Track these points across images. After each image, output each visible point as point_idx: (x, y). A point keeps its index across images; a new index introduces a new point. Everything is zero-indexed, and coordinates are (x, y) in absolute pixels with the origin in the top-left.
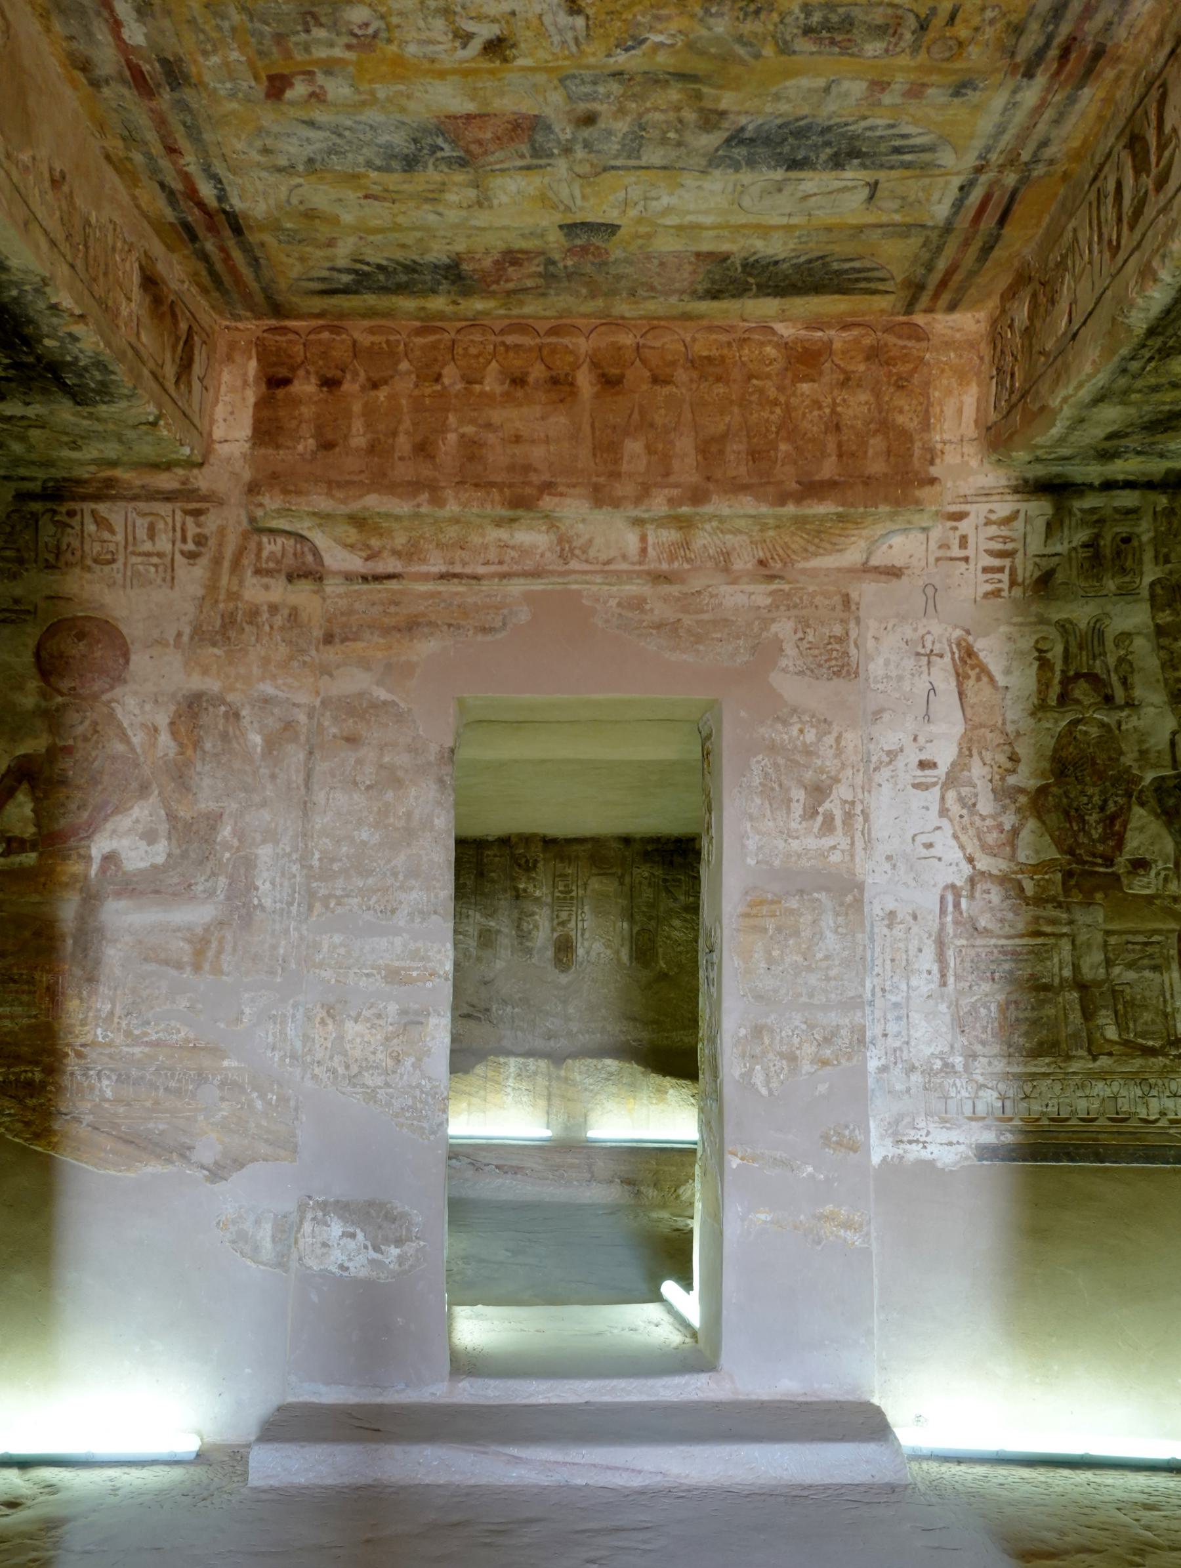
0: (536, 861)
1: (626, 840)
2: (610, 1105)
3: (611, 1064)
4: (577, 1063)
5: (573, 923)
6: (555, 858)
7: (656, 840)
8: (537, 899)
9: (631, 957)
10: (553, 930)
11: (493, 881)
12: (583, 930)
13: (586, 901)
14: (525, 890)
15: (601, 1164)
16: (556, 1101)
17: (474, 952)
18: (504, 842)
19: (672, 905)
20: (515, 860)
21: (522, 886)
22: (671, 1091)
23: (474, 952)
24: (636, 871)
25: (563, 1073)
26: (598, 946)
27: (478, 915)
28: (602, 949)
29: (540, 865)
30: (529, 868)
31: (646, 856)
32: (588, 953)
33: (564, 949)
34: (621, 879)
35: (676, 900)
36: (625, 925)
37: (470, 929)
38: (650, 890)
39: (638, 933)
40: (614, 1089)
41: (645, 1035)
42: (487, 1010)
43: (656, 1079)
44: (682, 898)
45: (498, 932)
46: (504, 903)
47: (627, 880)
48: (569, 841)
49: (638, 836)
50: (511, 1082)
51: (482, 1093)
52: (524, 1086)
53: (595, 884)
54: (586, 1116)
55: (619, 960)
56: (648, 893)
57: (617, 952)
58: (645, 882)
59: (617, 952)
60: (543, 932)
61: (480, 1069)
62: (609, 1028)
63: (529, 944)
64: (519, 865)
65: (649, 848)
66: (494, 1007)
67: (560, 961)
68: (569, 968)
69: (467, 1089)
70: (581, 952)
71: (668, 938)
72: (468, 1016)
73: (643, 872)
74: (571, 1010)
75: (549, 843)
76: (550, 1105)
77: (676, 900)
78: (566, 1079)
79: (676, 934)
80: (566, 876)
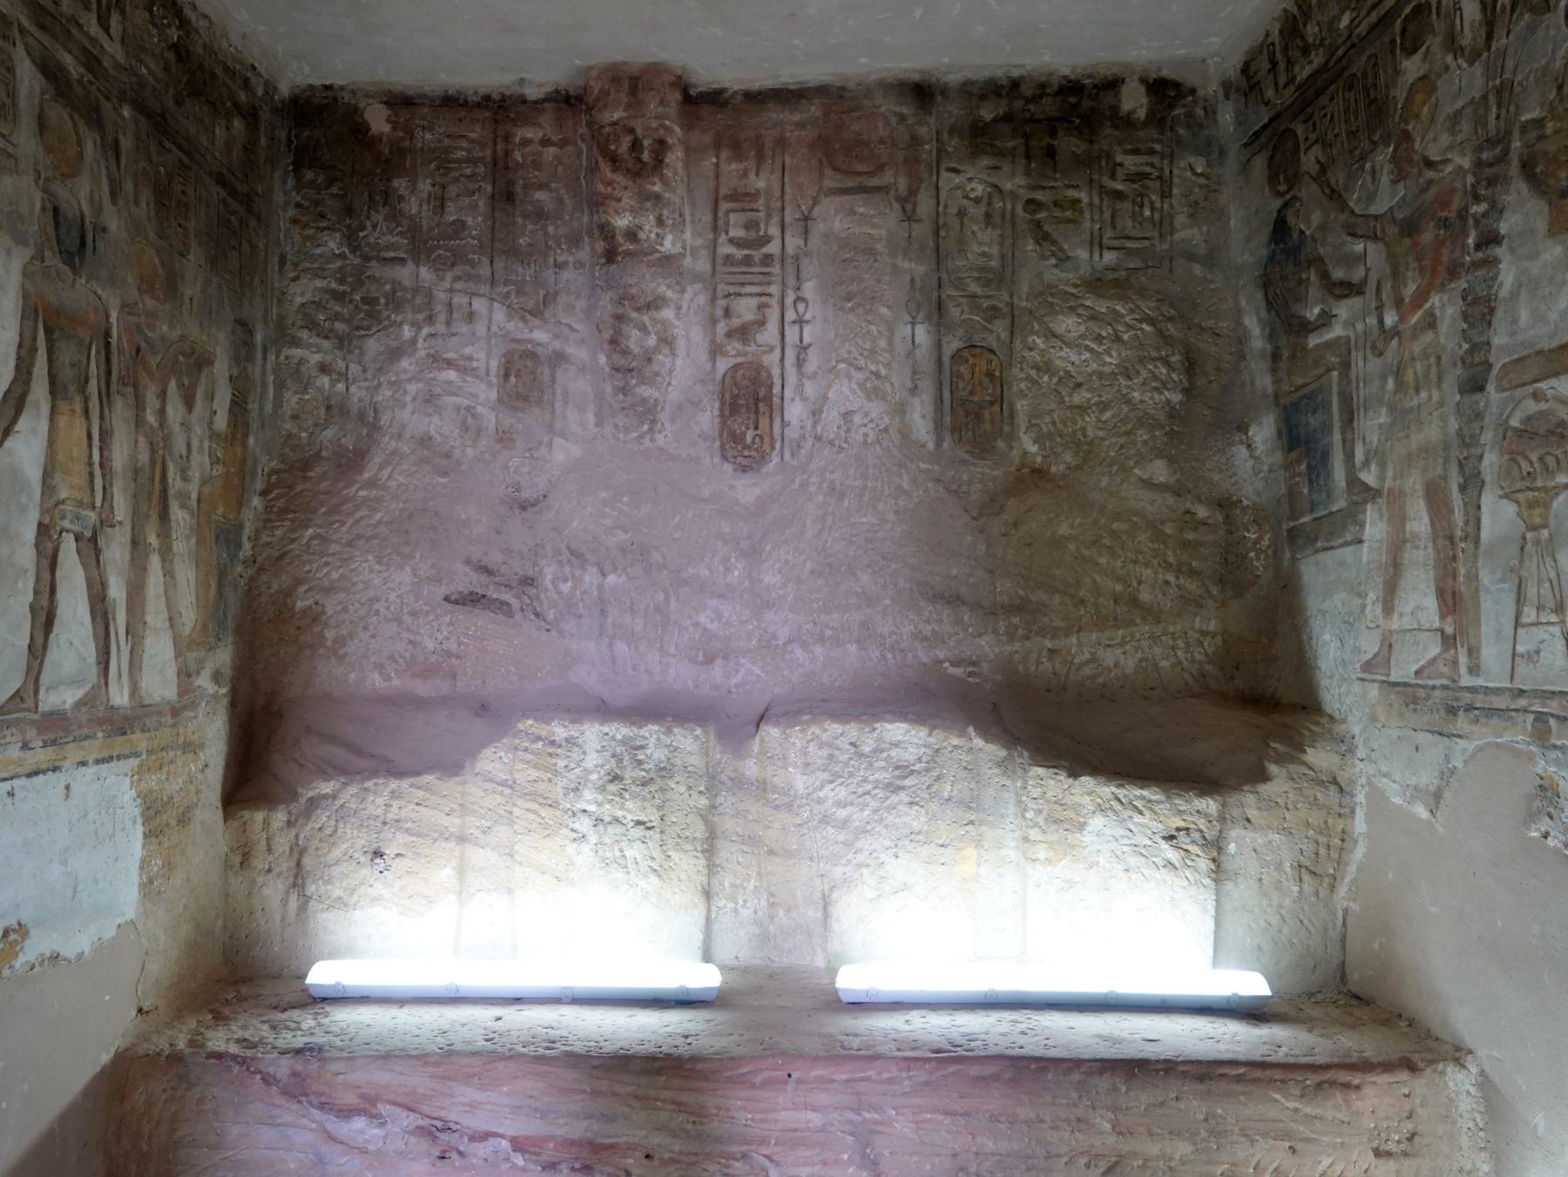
0: (661, 146)
1: (922, 92)
2: (904, 868)
3: (905, 738)
4: (797, 737)
5: (772, 328)
6: (717, 147)
7: (1008, 89)
8: (667, 260)
9: (938, 425)
10: (715, 351)
11: (540, 215)
12: (803, 349)
13: (809, 267)
14: (632, 235)
15: (902, 1126)
16: (729, 854)
17: (490, 419)
18: (569, 101)
19: (1053, 275)
20: (601, 142)
21: (622, 222)
22: (1097, 822)
23: (490, 419)
24: (948, 180)
25: (751, 768)
26: (845, 393)
27: (499, 314)
28: (857, 401)
29: (675, 157)
30: (641, 163)
31: (979, 138)
32: (816, 414)
33: (747, 404)
34: (907, 204)
35: (1064, 260)
36: (922, 334)
37: (477, 352)
38: (988, 235)
39: (957, 357)
40: (915, 819)
41: (987, 646)
42: (529, 581)
43: (1049, 784)
44: (1082, 254)
45: (559, 358)
46: (573, 276)
47: (925, 206)
48: (757, 98)
49: (954, 78)
50: (589, 800)
51: (503, 833)
52: (632, 810)
53: (834, 218)
54: (826, 904)
55: (905, 433)
56: (984, 244)
57: (901, 410)
58: (978, 211)
59: (901, 410)
60: (687, 357)
61: (493, 761)
62: (884, 627)
63: (646, 391)
64: (614, 160)
65: (987, 114)
66: (549, 572)
67: (737, 439)
68: (763, 458)
69: (452, 824)
70: (795, 411)
71: (1046, 367)
72: (473, 600)
73: (970, 181)
74: (771, 578)
75: (699, 102)
76: (712, 868)
77: (1064, 260)
78: (762, 787)
79: (1067, 358)
80: (754, 196)
